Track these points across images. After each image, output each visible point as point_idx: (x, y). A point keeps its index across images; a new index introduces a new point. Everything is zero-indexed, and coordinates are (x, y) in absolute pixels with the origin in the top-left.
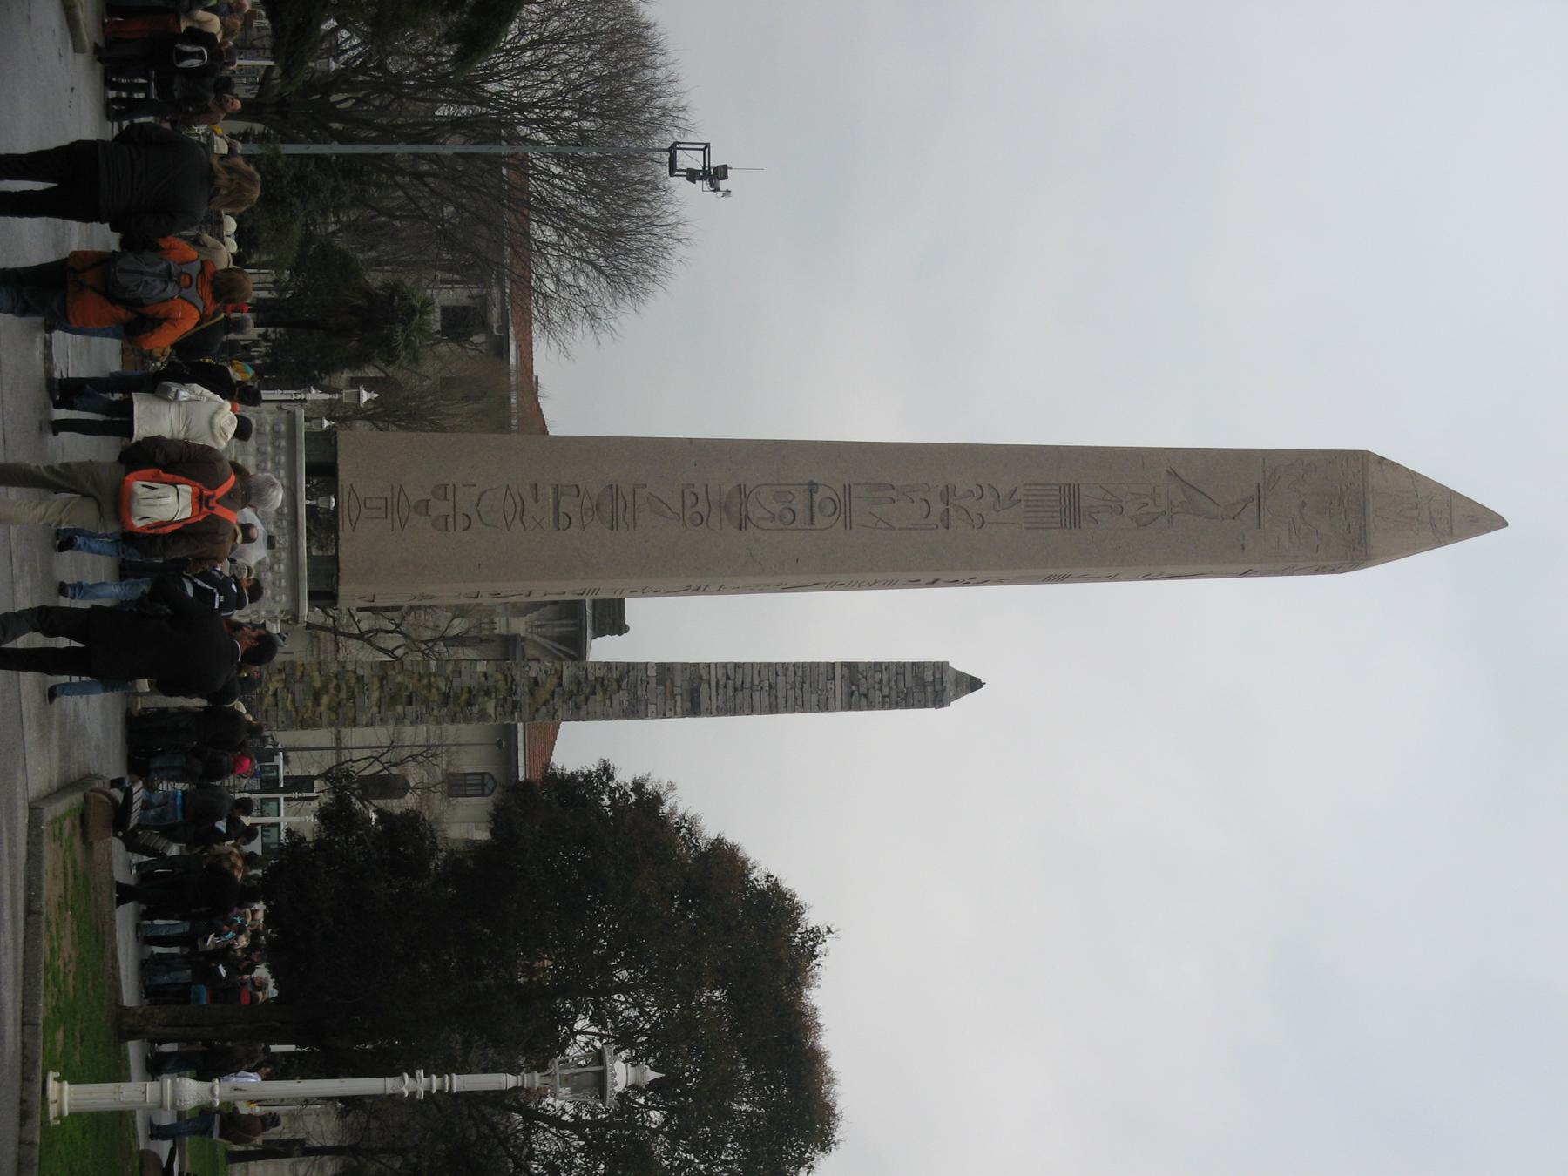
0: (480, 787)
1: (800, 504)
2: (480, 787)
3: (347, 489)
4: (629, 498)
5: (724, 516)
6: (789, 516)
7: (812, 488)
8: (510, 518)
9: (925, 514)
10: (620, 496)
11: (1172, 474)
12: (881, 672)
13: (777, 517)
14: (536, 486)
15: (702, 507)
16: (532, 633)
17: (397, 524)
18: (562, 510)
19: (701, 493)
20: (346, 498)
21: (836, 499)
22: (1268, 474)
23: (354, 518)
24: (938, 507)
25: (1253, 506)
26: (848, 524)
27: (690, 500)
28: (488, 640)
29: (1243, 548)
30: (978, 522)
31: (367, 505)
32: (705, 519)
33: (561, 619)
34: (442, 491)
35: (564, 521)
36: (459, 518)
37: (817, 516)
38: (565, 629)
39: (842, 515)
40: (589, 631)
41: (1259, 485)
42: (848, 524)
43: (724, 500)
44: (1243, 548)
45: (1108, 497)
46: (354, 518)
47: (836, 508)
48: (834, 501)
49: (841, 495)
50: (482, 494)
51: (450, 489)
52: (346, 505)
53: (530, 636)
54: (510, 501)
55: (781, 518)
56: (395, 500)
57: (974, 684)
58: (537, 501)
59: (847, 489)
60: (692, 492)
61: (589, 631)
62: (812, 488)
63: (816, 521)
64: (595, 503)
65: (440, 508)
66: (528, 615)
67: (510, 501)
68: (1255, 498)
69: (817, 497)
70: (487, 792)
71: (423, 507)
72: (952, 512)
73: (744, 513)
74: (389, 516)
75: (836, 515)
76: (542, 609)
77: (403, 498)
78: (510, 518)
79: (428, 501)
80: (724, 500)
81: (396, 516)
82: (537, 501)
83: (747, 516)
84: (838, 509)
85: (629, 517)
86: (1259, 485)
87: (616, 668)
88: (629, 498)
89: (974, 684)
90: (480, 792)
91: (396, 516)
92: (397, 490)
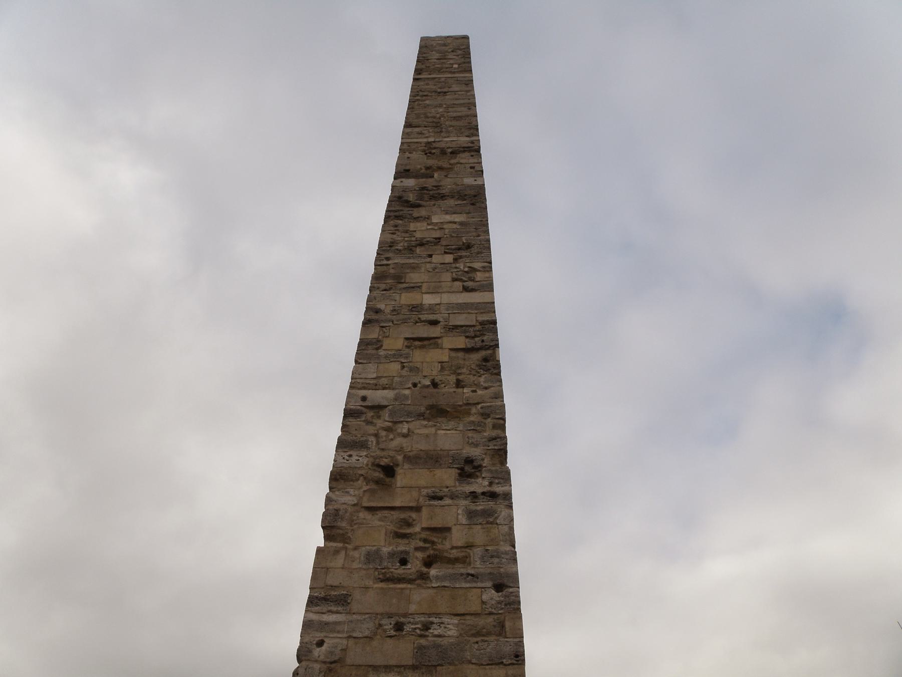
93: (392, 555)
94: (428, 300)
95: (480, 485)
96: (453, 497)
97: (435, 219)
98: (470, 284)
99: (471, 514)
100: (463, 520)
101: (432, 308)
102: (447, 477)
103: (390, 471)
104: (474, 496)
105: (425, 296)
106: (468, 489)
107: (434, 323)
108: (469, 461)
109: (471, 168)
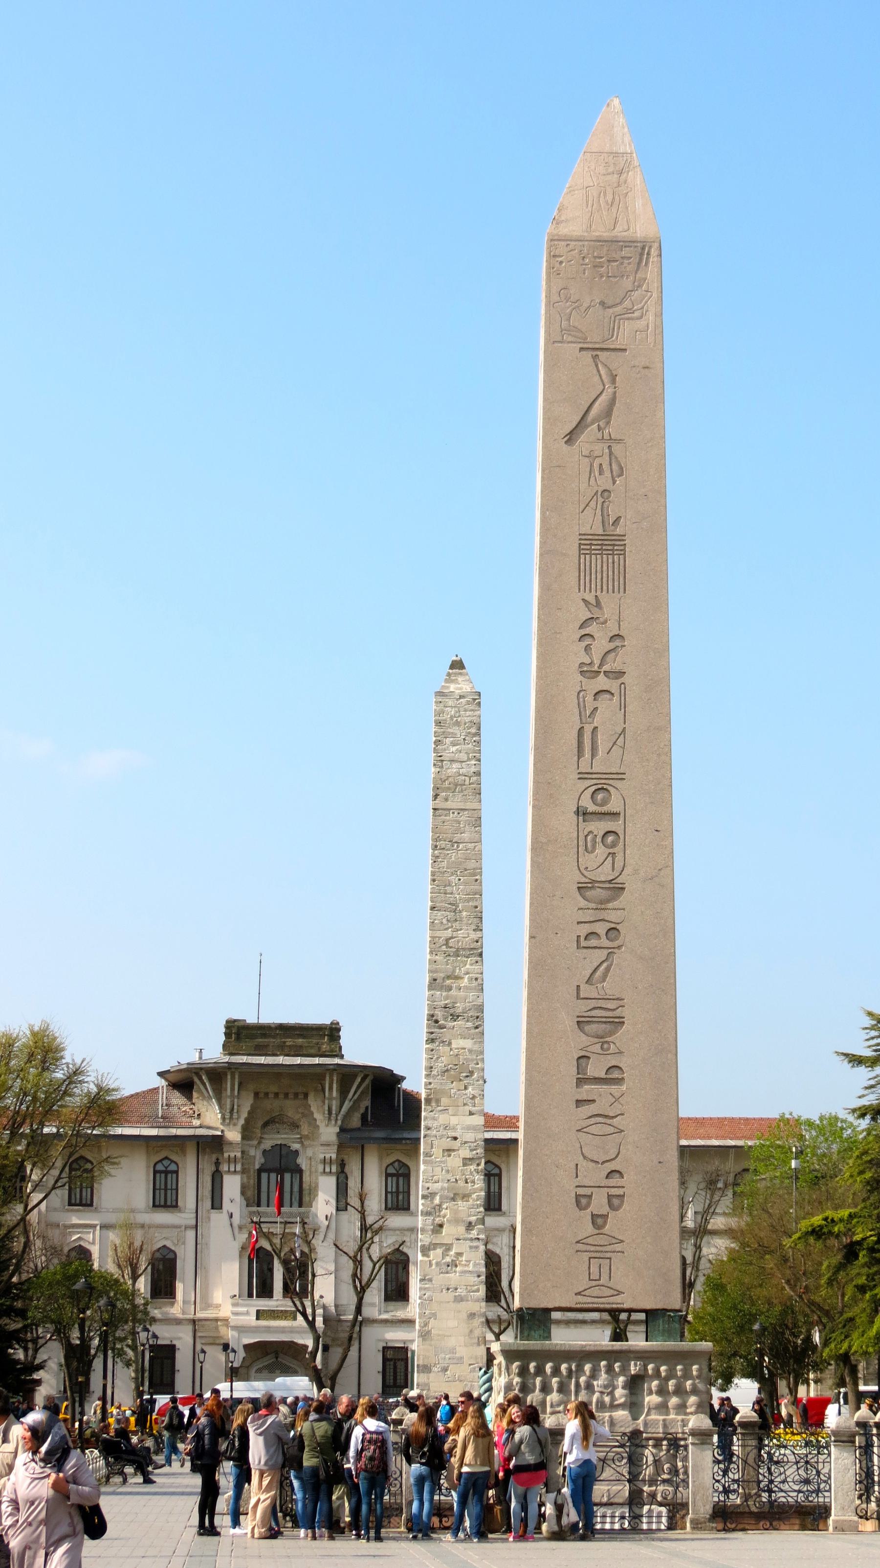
0: (492, 1178)
1: (599, 827)
2: (492, 1178)
3: (580, 1299)
4: (593, 1003)
5: (610, 905)
6: (610, 839)
7: (582, 813)
8: (612, 1130)
9: (608, 696)
10: (589, 1014)
11: (571, 437)
12: (442, 761)
13: (611, 851)
14: (577, 1101)
15: (601, 929)
16: (336, 1120)
17: (618, 1247)
18: (603, 1075)
19: (584, 930)
20: (590, 1300)
21: (593, 788)
22: (570, 339)
23: (612, 1292)
24: (602, 682)
25: (603, 355)
26: (620, 776)
27: (593, 942)
28: (342, 1165)
29: (647, 367)
30: (617, 643)
31: (598, 1278)
32: (613, 926)
33: (323, 1090)
34: (581, 1201)
35: (616, 1074)
36: (612, 1182)
37: (611, 807)
38: (335, 1086)
39: (610, 782)
40: (337, 1061)
41: (581, 349)
42: (620, 776)
43: (593, 905)
44: (647, 367)
45: (593, 504)
46: (612, 1292)
47: (602, 789)
48: (596, 790)
49: (588, 783)
50: (585, 1157)
51: (581, 1191)
52: (596, 1300)
53: (339, 1122)
54: (594, 1129)
55: (614, 845)
56: (593, 1248)
57: (457, 665)
58: (594, 1101)
59: (583, 776)
60: (586, 939)
61: (337, 1061)
62: (582, 813)
63: (615, 810)
64: (596, 1040)
65: (599, 1204)
66: (318, 1123)
67: (594, 1129)
68: (595, 353)
69: (592, 808)
70: (496, 1171)
71: (598, 1221)
72: (606, 668)
73: (607, 885)
74: (608, 1255)
75: (609, 788)
76: (312, 1109)
77: (590, 1241)
78: (611, 1130)
79: (593, 1215)
80: (593, 905)
81: (609, 1248)
82: (594, 1101)
83: (610, 882)
84: (605, 786)
85: (611, 1005)
86: (581, 349)
87: (432, 1033)
88: (593, 1003)
89: (457, 665)
90: (497, 1178)
91: (609, 1248)
92: (580, 1247)
93: (445, 1263)
94: (454, 1120)
95: (474, 1233)
96: (465, 1239)
97: (454, 1046)
98: (473, 1109)
99: (471, 1247)
100: (468, 1249)
101: (454, 1129)
102: (461, 1229)
103: (441, 1226)
104: (471, 1240)
105: (452, 1118)
106: (471, 1236)
107: (455, 1138)
108: (470, 1223)
109: (476, 979)
